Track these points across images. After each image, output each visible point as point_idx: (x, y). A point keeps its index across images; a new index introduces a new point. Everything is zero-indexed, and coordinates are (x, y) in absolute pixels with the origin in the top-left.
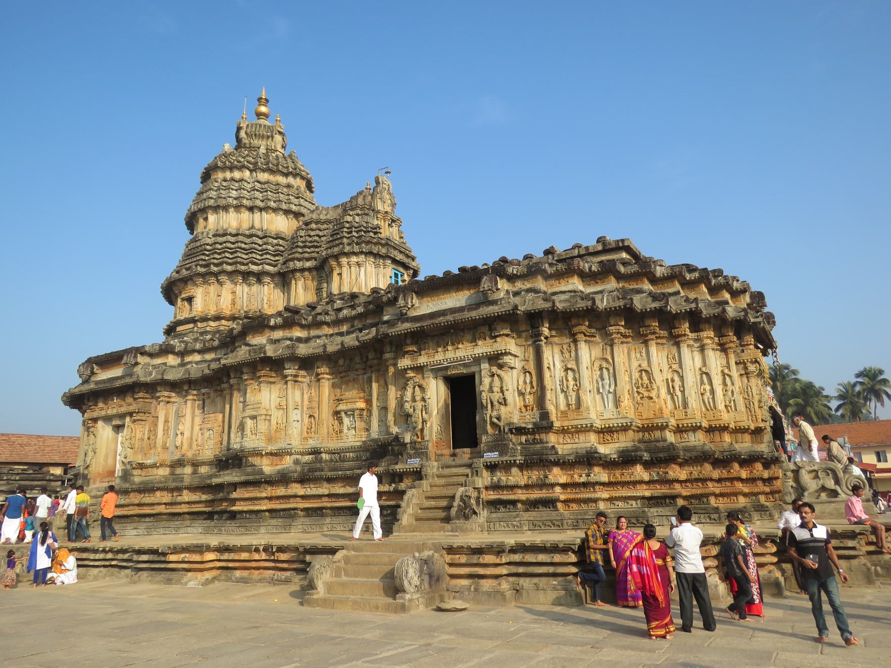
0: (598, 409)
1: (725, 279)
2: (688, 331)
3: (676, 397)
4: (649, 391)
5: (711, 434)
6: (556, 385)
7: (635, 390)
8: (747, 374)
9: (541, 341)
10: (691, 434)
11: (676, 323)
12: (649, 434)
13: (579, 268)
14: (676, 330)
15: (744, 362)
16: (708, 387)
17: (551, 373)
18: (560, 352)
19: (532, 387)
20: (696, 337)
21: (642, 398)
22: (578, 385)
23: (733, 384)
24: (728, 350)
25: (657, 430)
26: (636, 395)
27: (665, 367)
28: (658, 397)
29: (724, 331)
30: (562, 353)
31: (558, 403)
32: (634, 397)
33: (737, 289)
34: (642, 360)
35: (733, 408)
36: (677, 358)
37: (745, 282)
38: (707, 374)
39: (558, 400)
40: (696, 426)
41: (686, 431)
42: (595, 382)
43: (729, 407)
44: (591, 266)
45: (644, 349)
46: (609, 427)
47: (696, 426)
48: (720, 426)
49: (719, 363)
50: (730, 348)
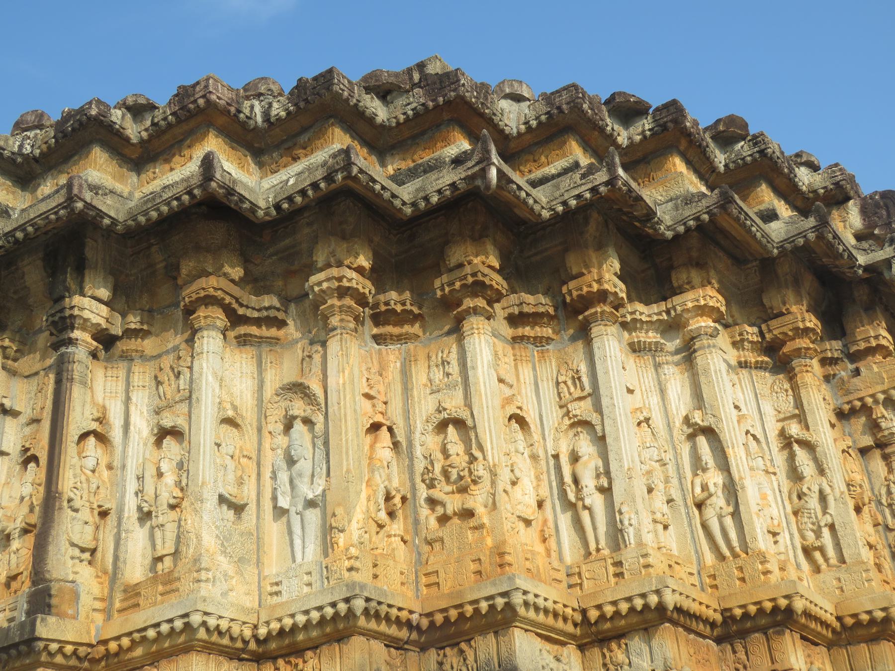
0: (266, 572)
1: (755, 144)
2: (621, 290)
3: (585, 516)
4: (463, 490)
5: (739, 647)
6: (123, 496)
7: (423, 493)
8: (881, 445)
9: (71, 342)
10: (636, 643)
11: (573, 263)
12: (462, 652)
13: (208, 102)
14: (572, 284)
15: (864, 406)
16: (715, 479)
17: (112, 454)
18: (153, 383)
19: (32, 510)
20: (665, 316)
21: (443, 519)
22: (184, 484)
23: (821, 472)
24: (795, 363)
25: (483, 631)
26: (425, 511)
27: (553, 416)
28: (494, 506)
29: (772, 300)
30: (159, 383)
31: (122, 556)
32: (416, 522)
33: (815, 192)
34: (448, 386)
35: (831, 552)
36: (585, 380)
37: (836, 165)
38: (709, 432)
39: (122, 548)
40: (646, 606)
41: (619, 636)
42: (267, 474)
43: (817, 555)
44: (270, 105)
45: (454, 345)
46: (282, 632)
47: (646, 606)
48: (761, 611)
49: (768, 409)
50: (798, 353)
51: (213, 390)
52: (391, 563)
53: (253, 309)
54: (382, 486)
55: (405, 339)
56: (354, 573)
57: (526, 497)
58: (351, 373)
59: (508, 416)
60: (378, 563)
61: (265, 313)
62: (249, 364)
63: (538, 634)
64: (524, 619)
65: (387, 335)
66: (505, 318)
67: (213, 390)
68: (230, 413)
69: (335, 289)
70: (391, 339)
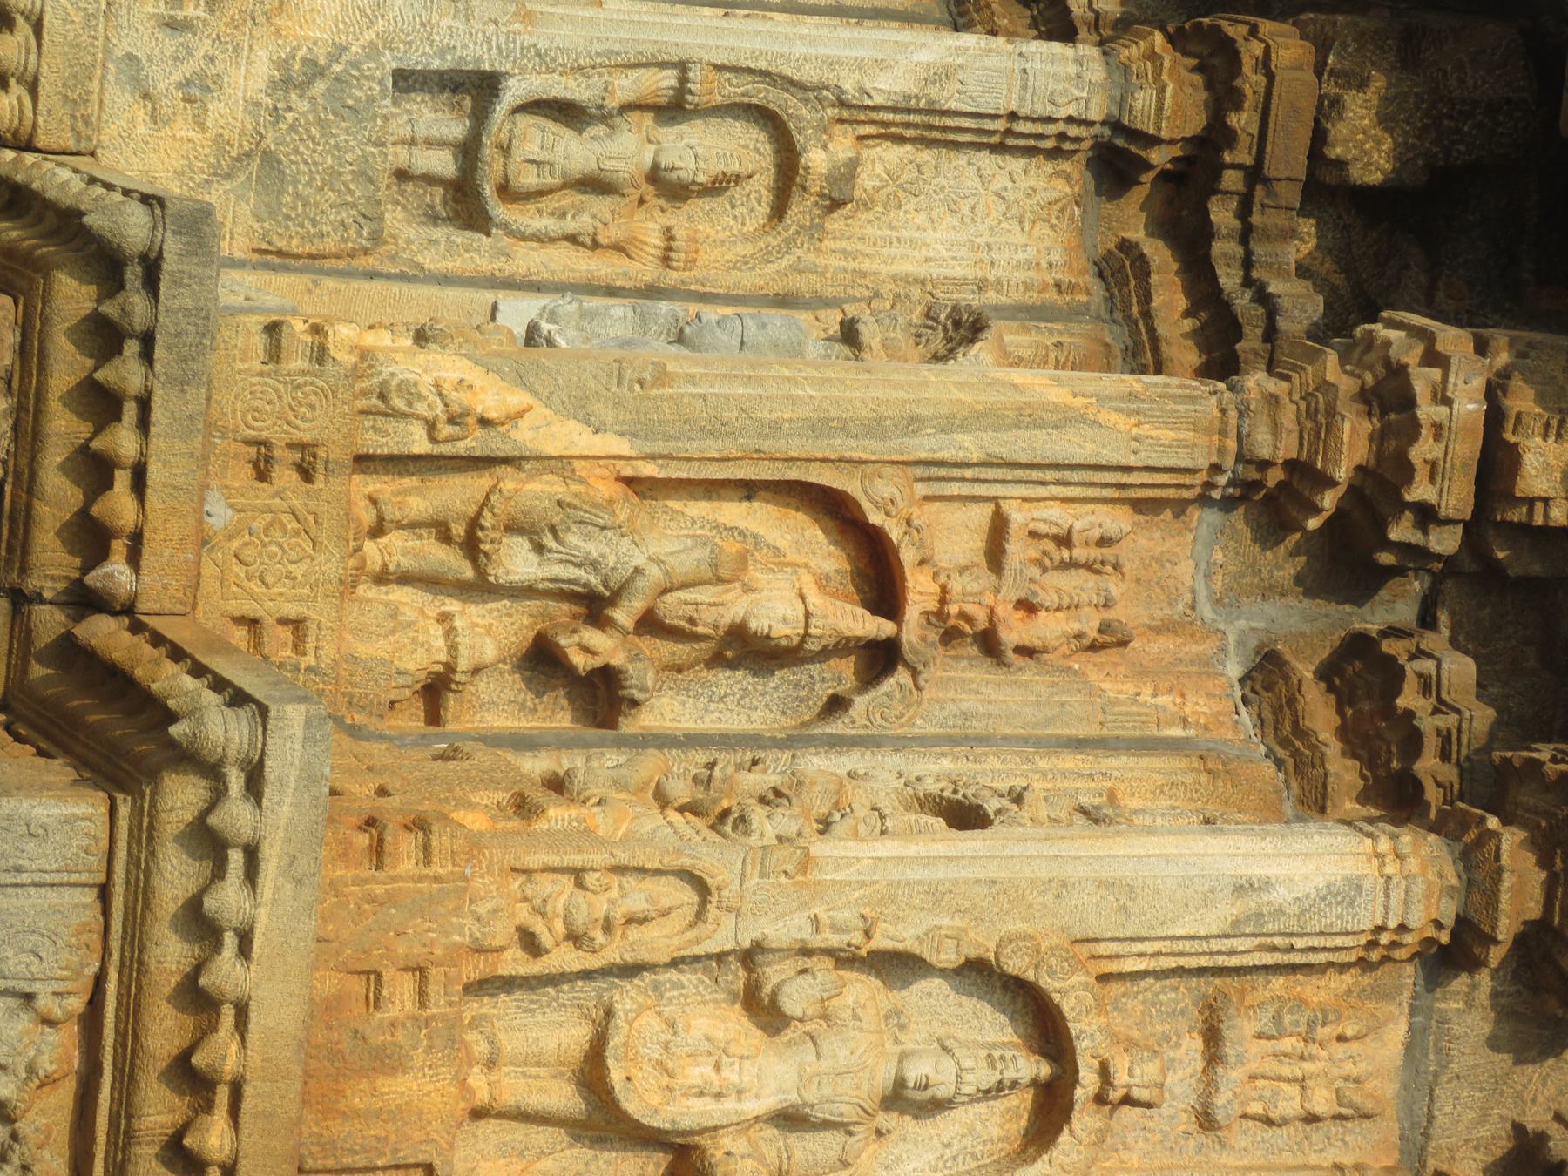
51: (881, 65)
52: (331, 565)
53: (1247, 263)
54: (639, 560)
55: (1296, 754)
56: (259, 341)
57: (708, 1071)
58: (1065, 419)
59: (1048, 984)
60: (319, 483)
61: (1243, 302)
62: (1033, 274)
63: (100, 980)
64: (150, 839)
65: (1286, 678)
66: (1518, 1128)
67: (881, 65)
68: (817, 160)
69: (1387, 362)
70: (1277, 711)
